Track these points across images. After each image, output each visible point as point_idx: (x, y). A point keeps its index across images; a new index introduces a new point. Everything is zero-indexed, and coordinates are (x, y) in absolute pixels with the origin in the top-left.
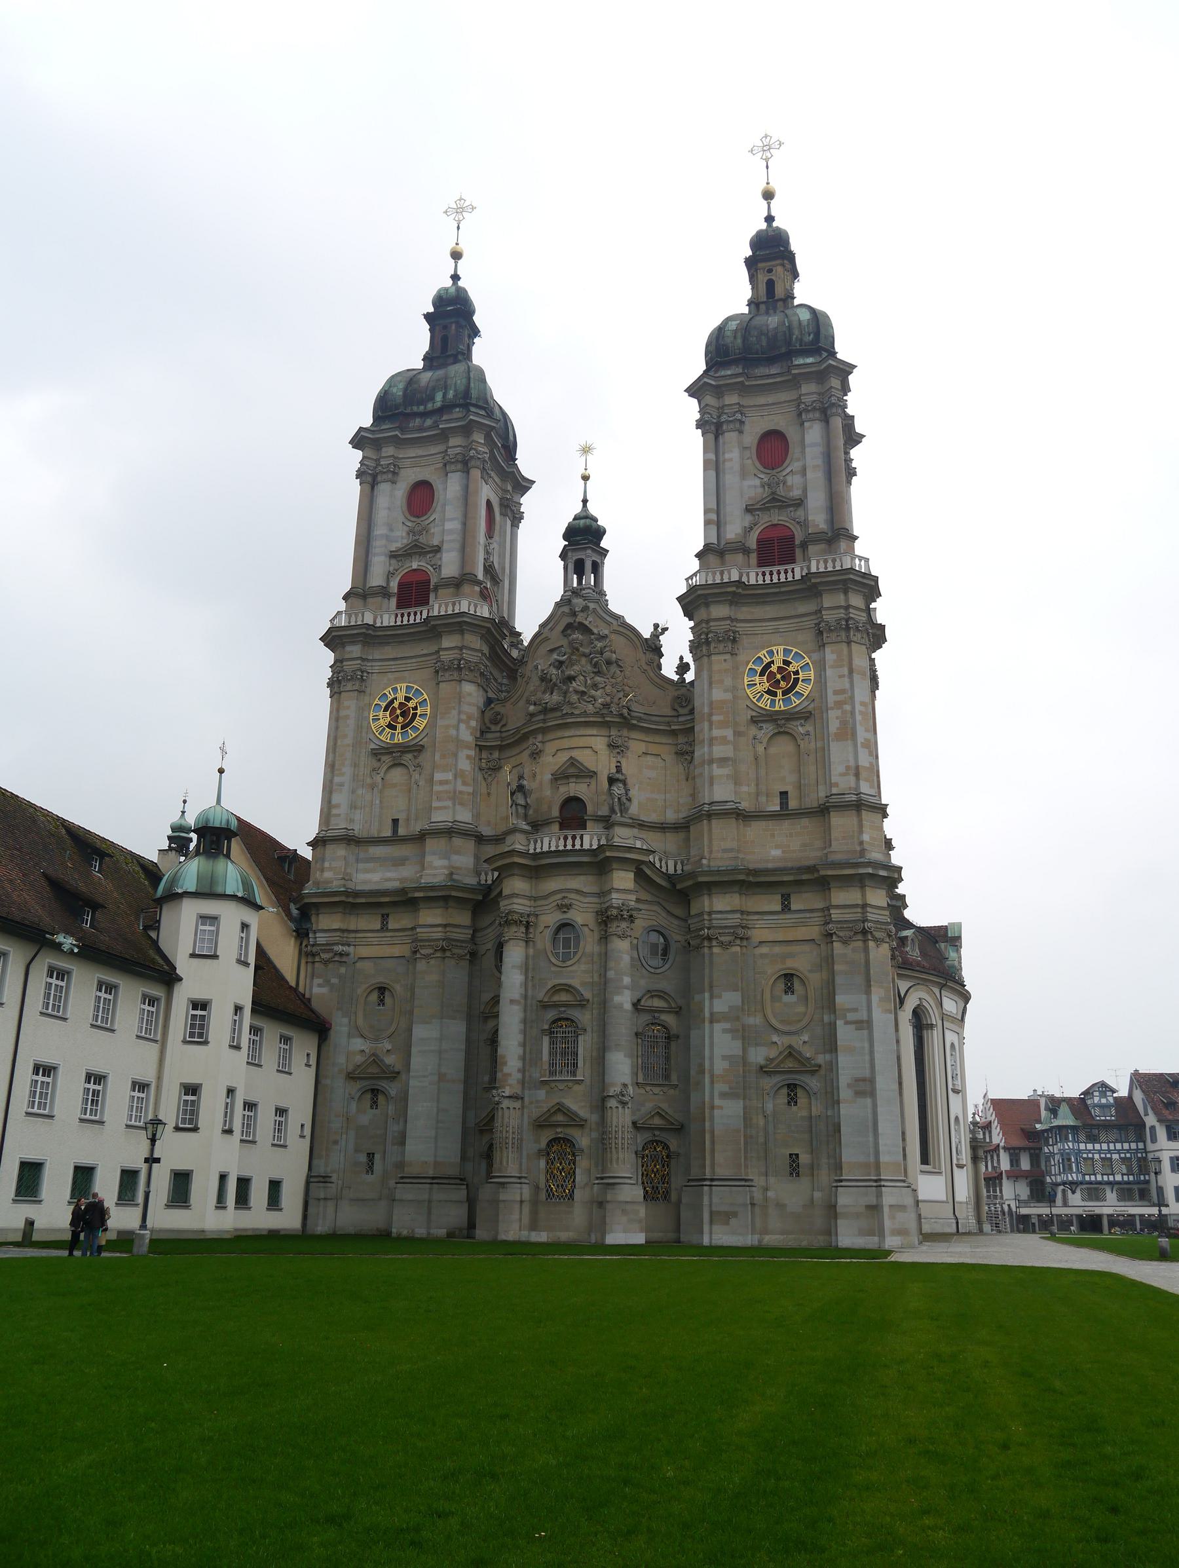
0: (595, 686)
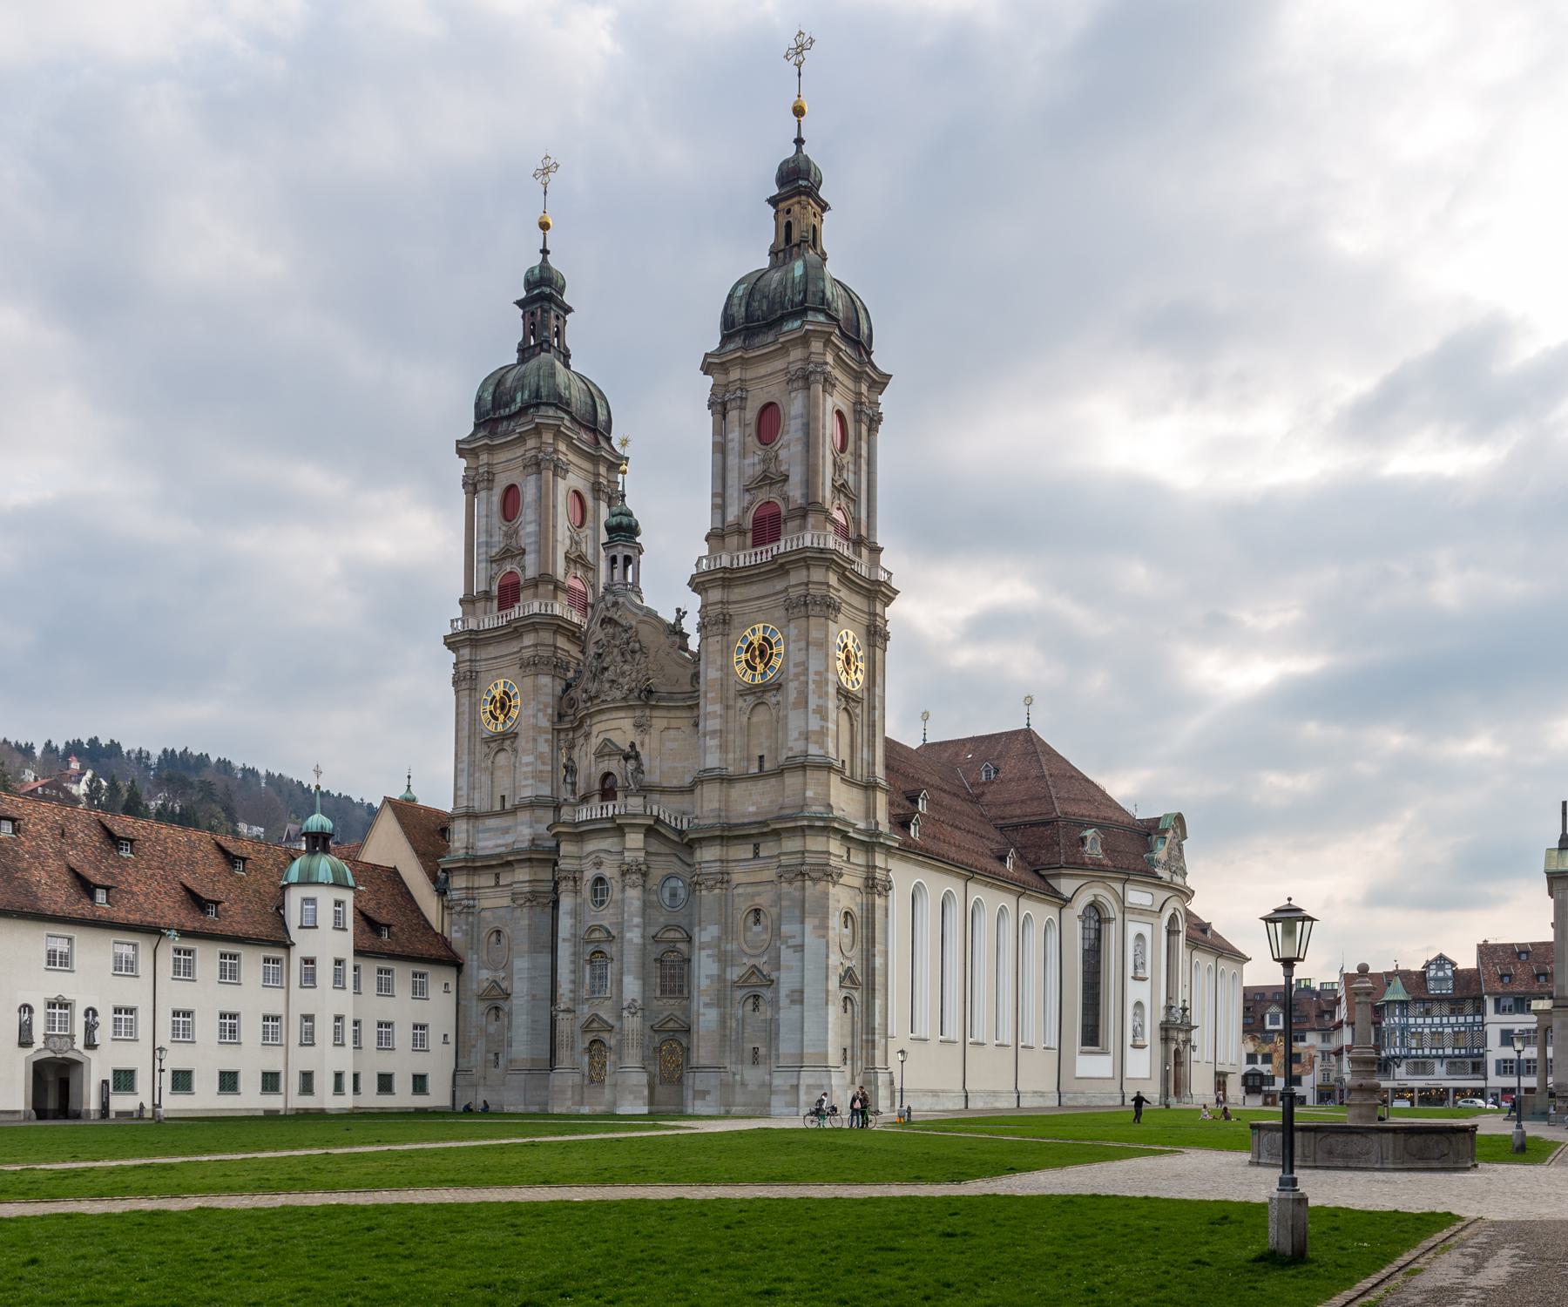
0: (623, 674)
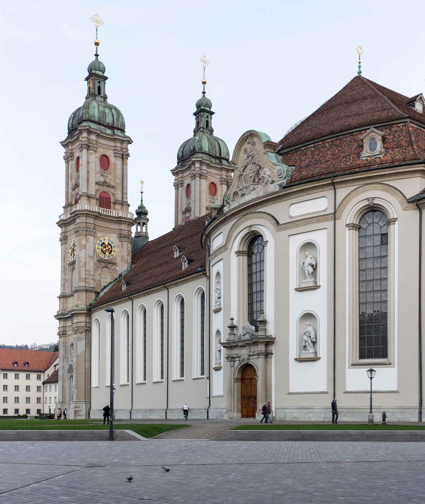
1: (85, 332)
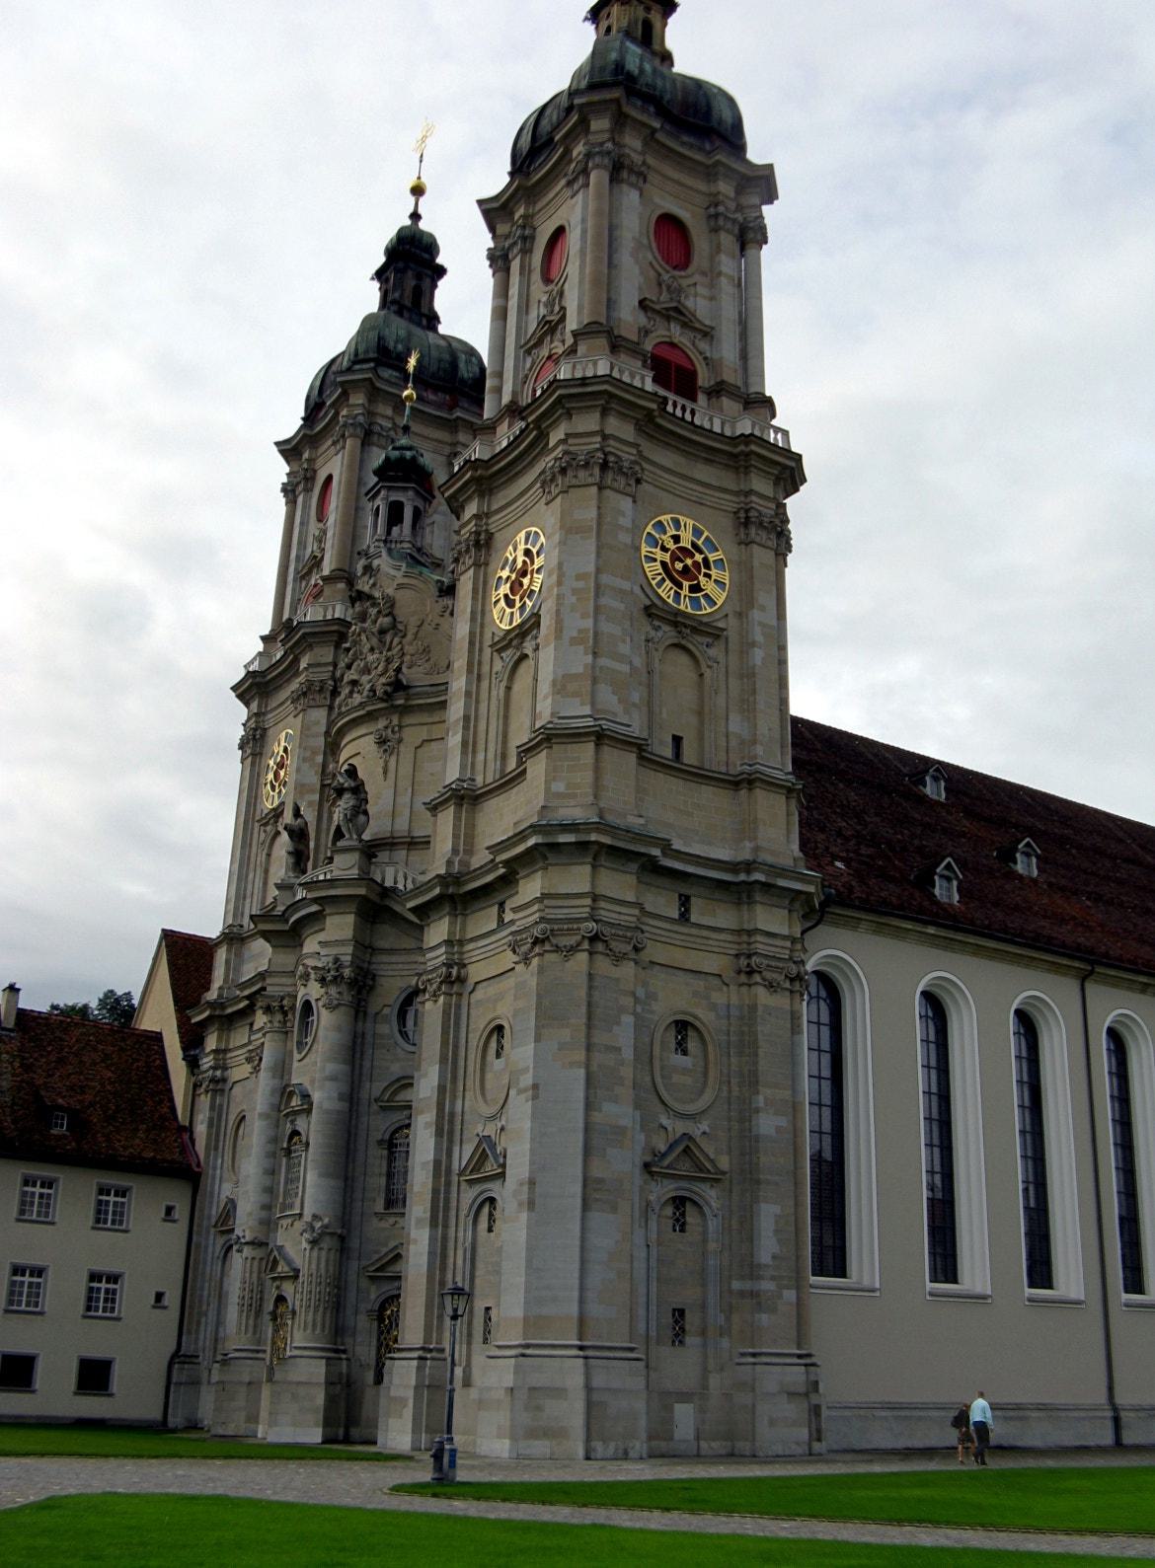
0: (367, 670)
1: (586, 945)
